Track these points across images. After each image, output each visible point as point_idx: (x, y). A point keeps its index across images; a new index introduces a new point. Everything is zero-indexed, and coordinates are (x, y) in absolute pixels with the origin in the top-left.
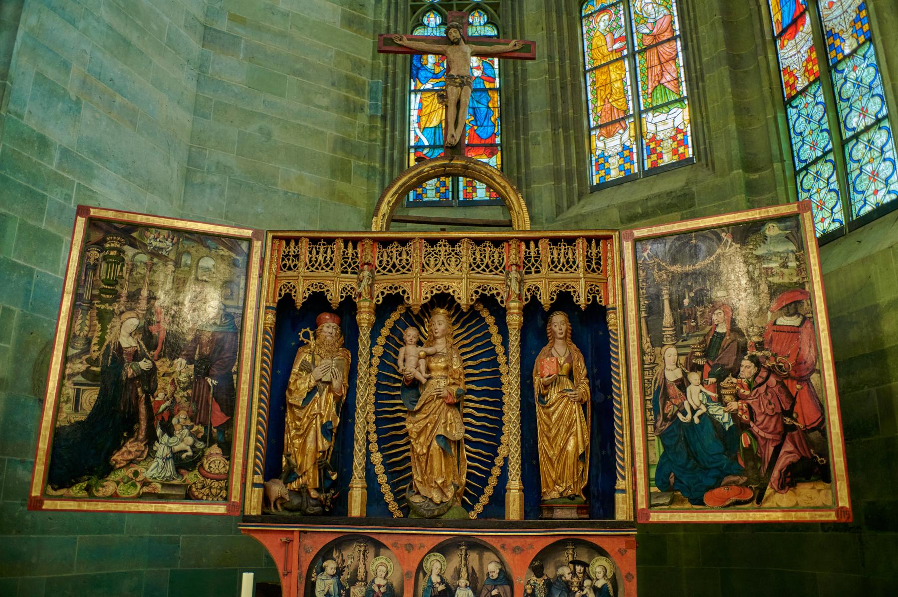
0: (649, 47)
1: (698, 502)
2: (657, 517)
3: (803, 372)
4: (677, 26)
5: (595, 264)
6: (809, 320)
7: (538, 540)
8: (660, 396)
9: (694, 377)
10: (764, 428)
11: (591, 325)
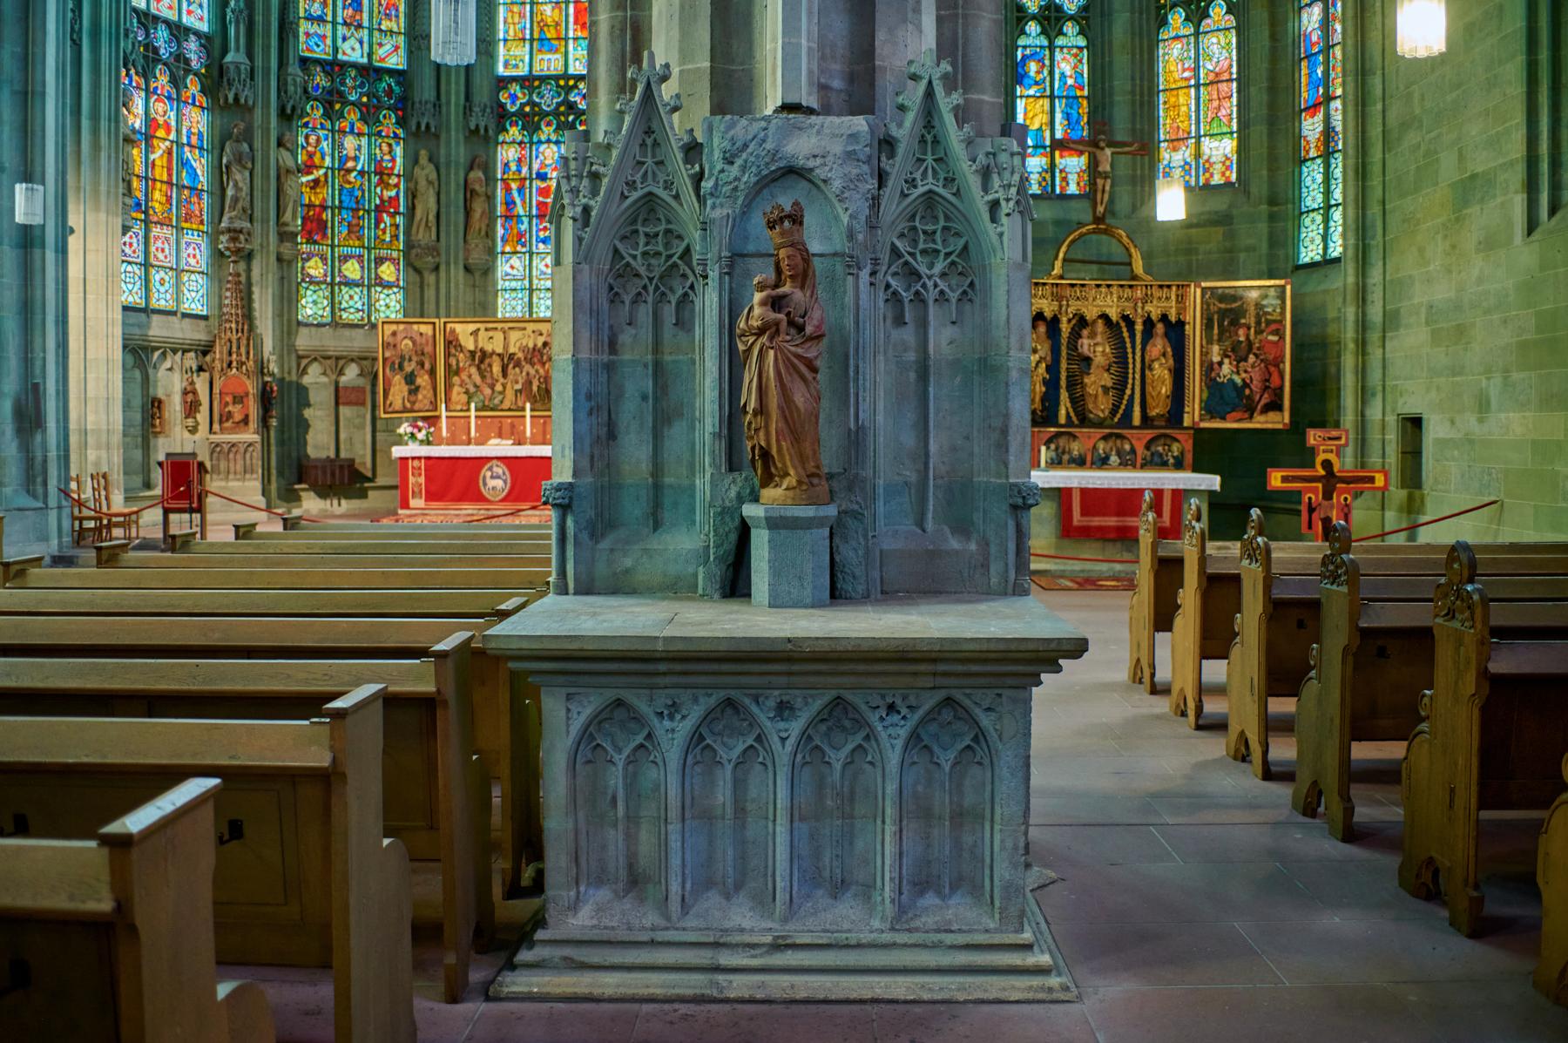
0: (1212, 83)
1: (1223, 418)
2: (1204, 425)
3: (1278, 361)
4: (1234, 70)
5: (1181, 299)
6: (1282, 338)
7: (1149, 434)
8: (1209, 368)
9: (1226, 361)
10: (1256, 385)
11: (1176, 331)
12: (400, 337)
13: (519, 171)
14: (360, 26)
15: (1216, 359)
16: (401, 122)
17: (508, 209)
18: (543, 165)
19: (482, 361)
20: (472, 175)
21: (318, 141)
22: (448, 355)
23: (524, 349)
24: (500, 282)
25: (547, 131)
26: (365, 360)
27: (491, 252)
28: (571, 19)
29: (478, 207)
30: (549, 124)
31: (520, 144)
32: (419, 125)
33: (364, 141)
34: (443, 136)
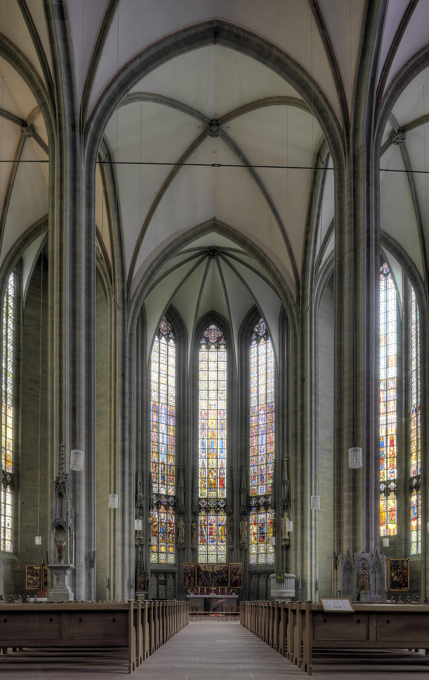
12: (188, 567)
13: (205, 523)
14: (165, 484)
15: (393, 576)
16: (174, 510)
17: (202, 533)
18: (211, 521)
19: (206, 574)
20: (193, 524)
21: (155, 515)
22: (198, 572)
23: (217, 571)
24: (199, 552)
25: (212, 513)
26: (166, 573)
27: (198, 545)
28: (218, 483)
29: (195, 532)
30: (213, 511)
31: (205, 516)
32: (180, 511)
33: (166, 515)
34: (186, 514)
